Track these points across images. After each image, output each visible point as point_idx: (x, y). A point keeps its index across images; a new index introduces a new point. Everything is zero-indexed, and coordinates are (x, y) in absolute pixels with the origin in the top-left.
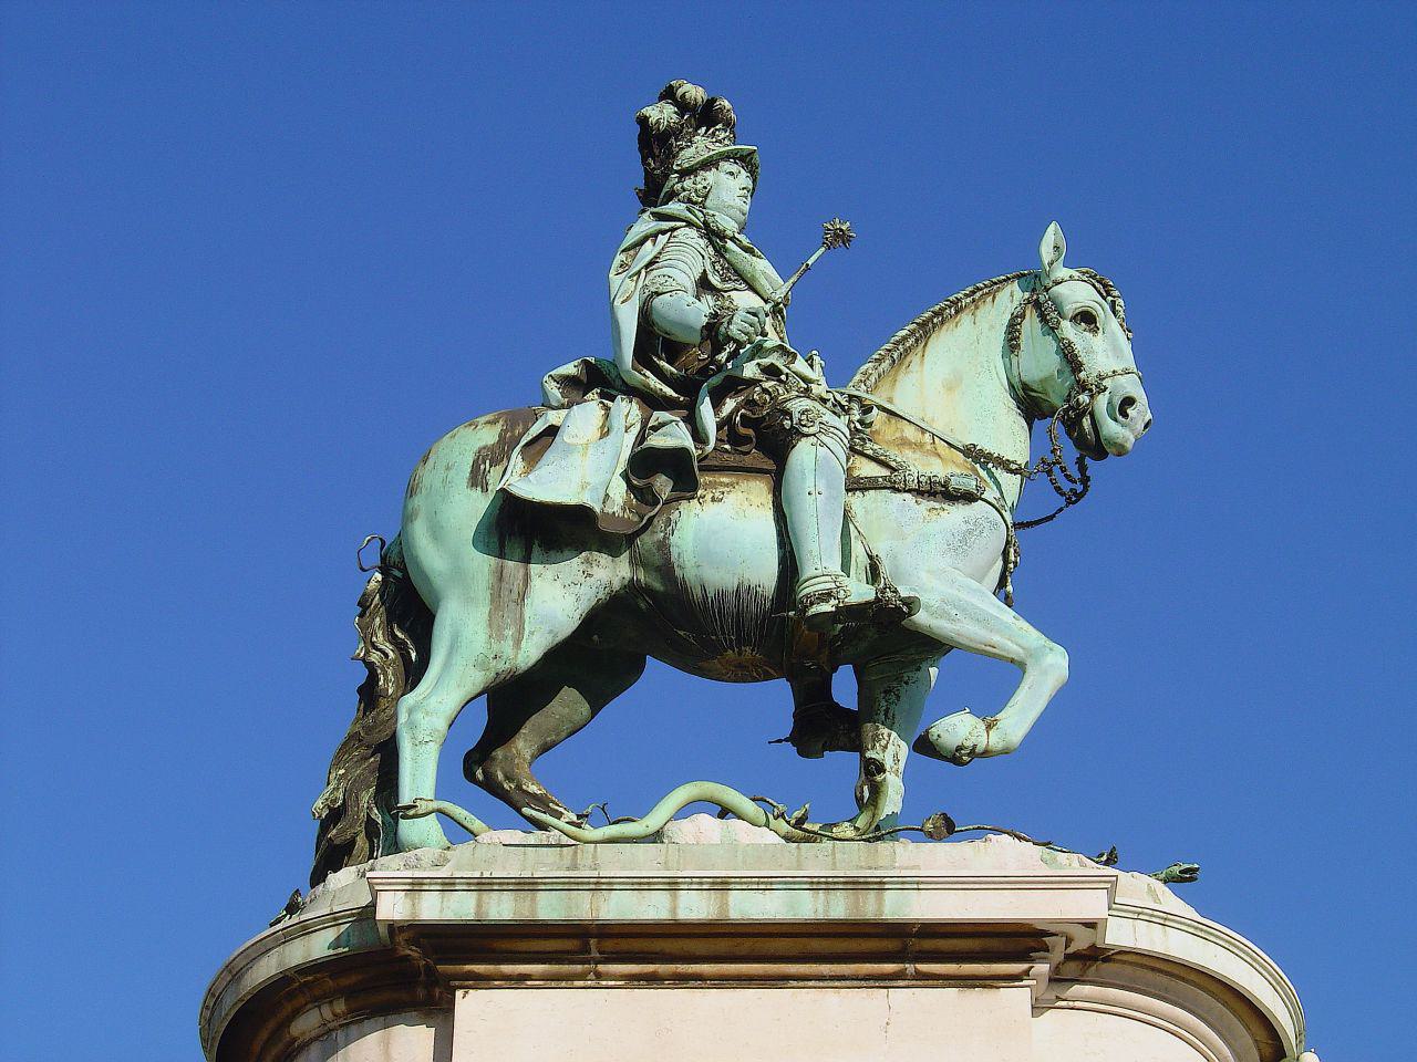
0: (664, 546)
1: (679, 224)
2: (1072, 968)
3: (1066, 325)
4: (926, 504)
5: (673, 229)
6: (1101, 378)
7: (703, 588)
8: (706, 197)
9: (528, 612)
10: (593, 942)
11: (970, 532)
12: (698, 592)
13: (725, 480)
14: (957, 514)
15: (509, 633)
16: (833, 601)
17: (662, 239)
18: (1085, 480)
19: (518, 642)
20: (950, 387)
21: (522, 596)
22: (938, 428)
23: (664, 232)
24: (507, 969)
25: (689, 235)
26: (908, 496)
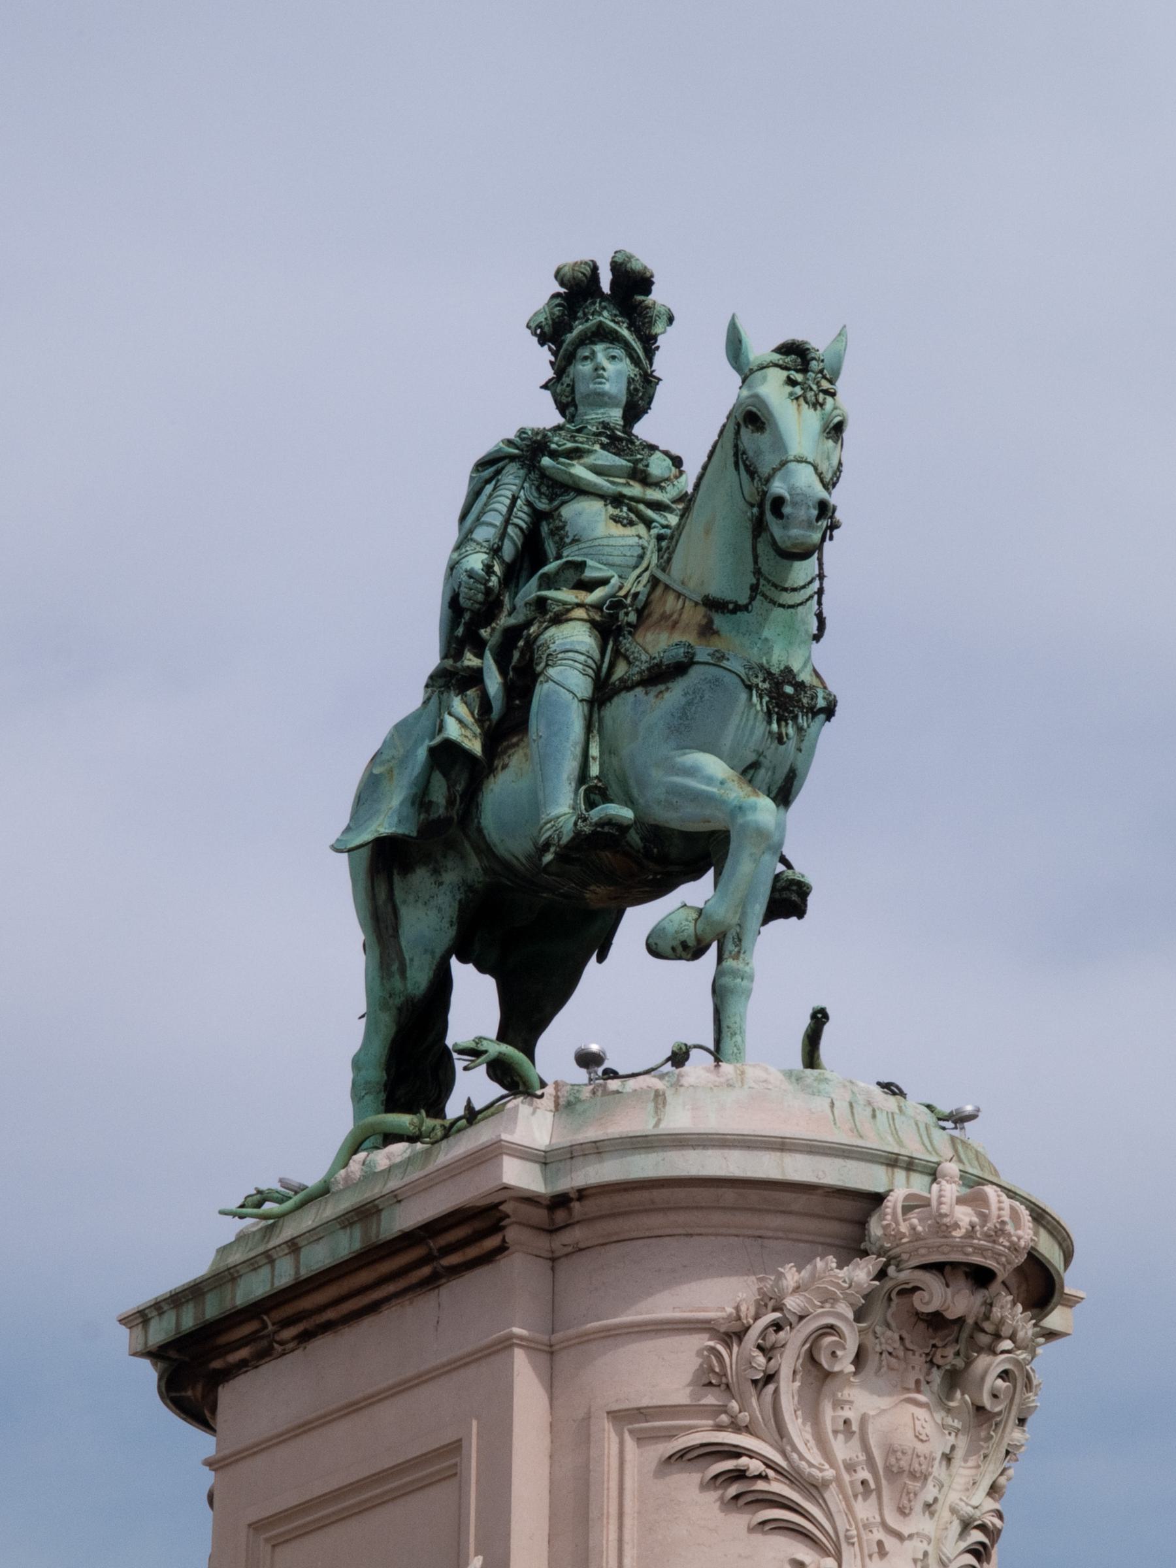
0: (480, 830)
1: (501, 464)
2: (560, 1216)
4: (654, 691)
5: (498, 472)
7: (517, 859)
8: (573, 391)
9: (403, 944)
10: (265, 1318)
11: (690, 703)
12: (515, 862)
13: (515, 740)
14: (676, 693)
15: (395, 967)
16: (552, 849)
18: (821, 576)
19: (403, 972)
20: (707, 532)
21: (396, 929)
23: (488, 481)
24: (234, 1358)
26: (639, 691)
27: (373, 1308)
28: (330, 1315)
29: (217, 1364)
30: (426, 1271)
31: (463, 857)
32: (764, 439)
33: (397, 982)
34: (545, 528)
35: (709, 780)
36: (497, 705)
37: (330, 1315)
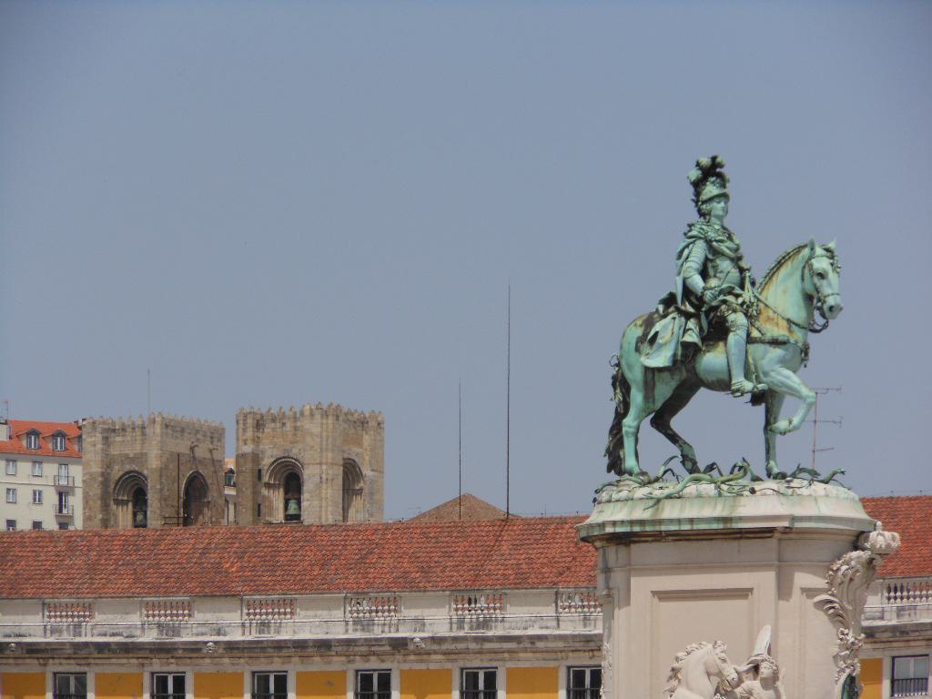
0: (694, 368)
3: (816, 279)
5: (694, 242)
6: (825, 297)
13: (711, 343)
17: (691, 246)
21: (653, 389)
22: (779, 310)
24: (642, 539)
25: (700, 245)
27: (711, 539)
28: (692, 537)
29: (634, 539)
30: (738, 536)
31: (680, 371)
32: (824, 282)
33: (651, 405)
34: (710, 265)
35: (794, 382)
36: (706, 331)
37: (692, 537)
